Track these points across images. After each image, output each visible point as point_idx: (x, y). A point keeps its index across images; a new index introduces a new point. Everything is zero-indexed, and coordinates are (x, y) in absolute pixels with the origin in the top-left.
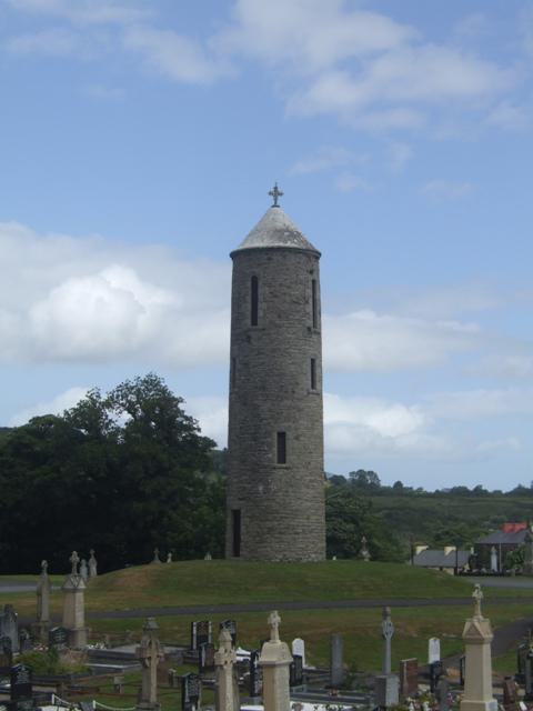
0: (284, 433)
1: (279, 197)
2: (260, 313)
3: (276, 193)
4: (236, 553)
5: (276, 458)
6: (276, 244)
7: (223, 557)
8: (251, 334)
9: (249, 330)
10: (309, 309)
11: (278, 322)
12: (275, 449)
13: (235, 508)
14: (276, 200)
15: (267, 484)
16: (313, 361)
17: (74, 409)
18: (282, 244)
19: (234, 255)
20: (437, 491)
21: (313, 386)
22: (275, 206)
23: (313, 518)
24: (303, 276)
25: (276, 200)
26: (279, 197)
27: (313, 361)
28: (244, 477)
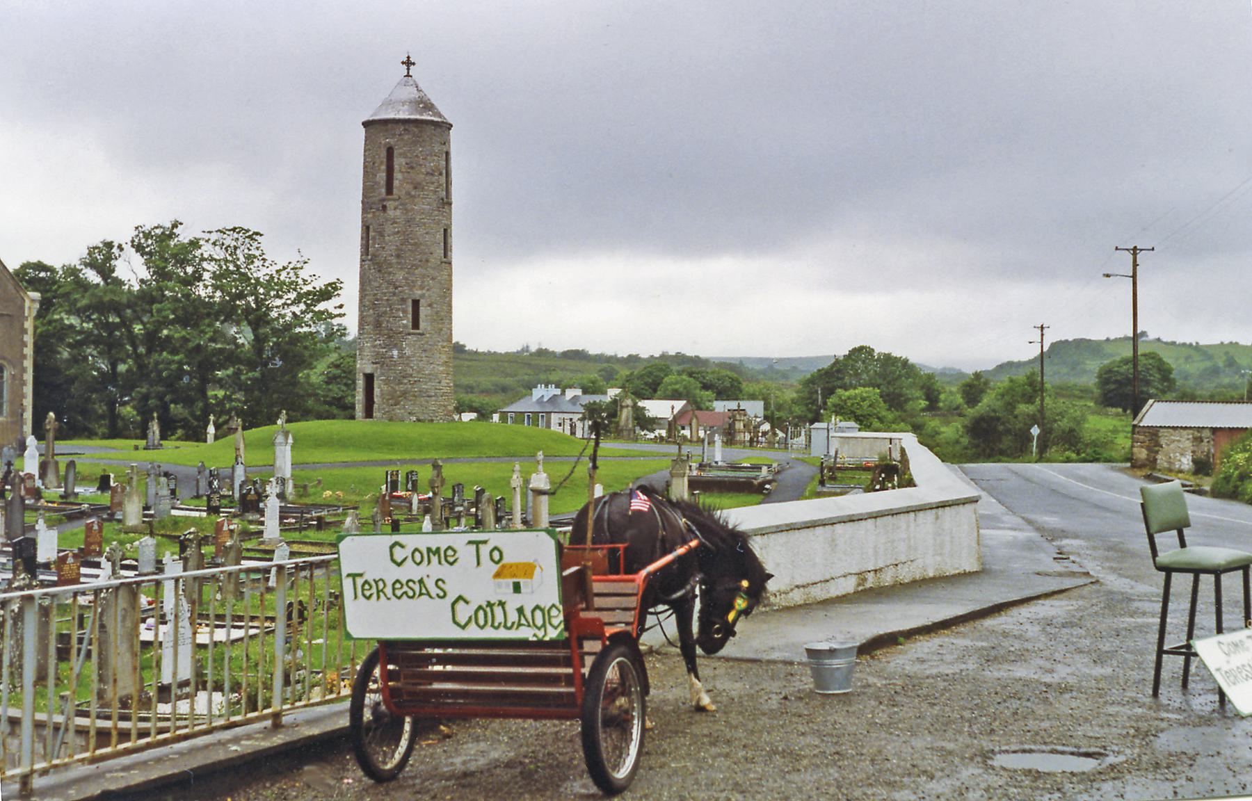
0: (419, 301)
1: (412, 67)
2: (396, 183)
3: (408, 63)
4: (369, 413)
5: (410, 325)
6: (413, 117)
7: (353, 417)
8: (388, 204)
9: (384, 200)
10: (443, 179)
11: (413, 193)
12: (410, 316)
13: (368, 371)
14: (408, 69)
15: (401, 350)
16: (445, 231)
17: (113, 271)
18: (418, 117)
19: (366, 124)
20: (630, 356)
21: (445, 256)
22: (408, 75)
23: (444, 382)
24: (437, 148)
25: (408, 69)
26: (412, 67)
27: (445, 231)
28: (378, 342)
